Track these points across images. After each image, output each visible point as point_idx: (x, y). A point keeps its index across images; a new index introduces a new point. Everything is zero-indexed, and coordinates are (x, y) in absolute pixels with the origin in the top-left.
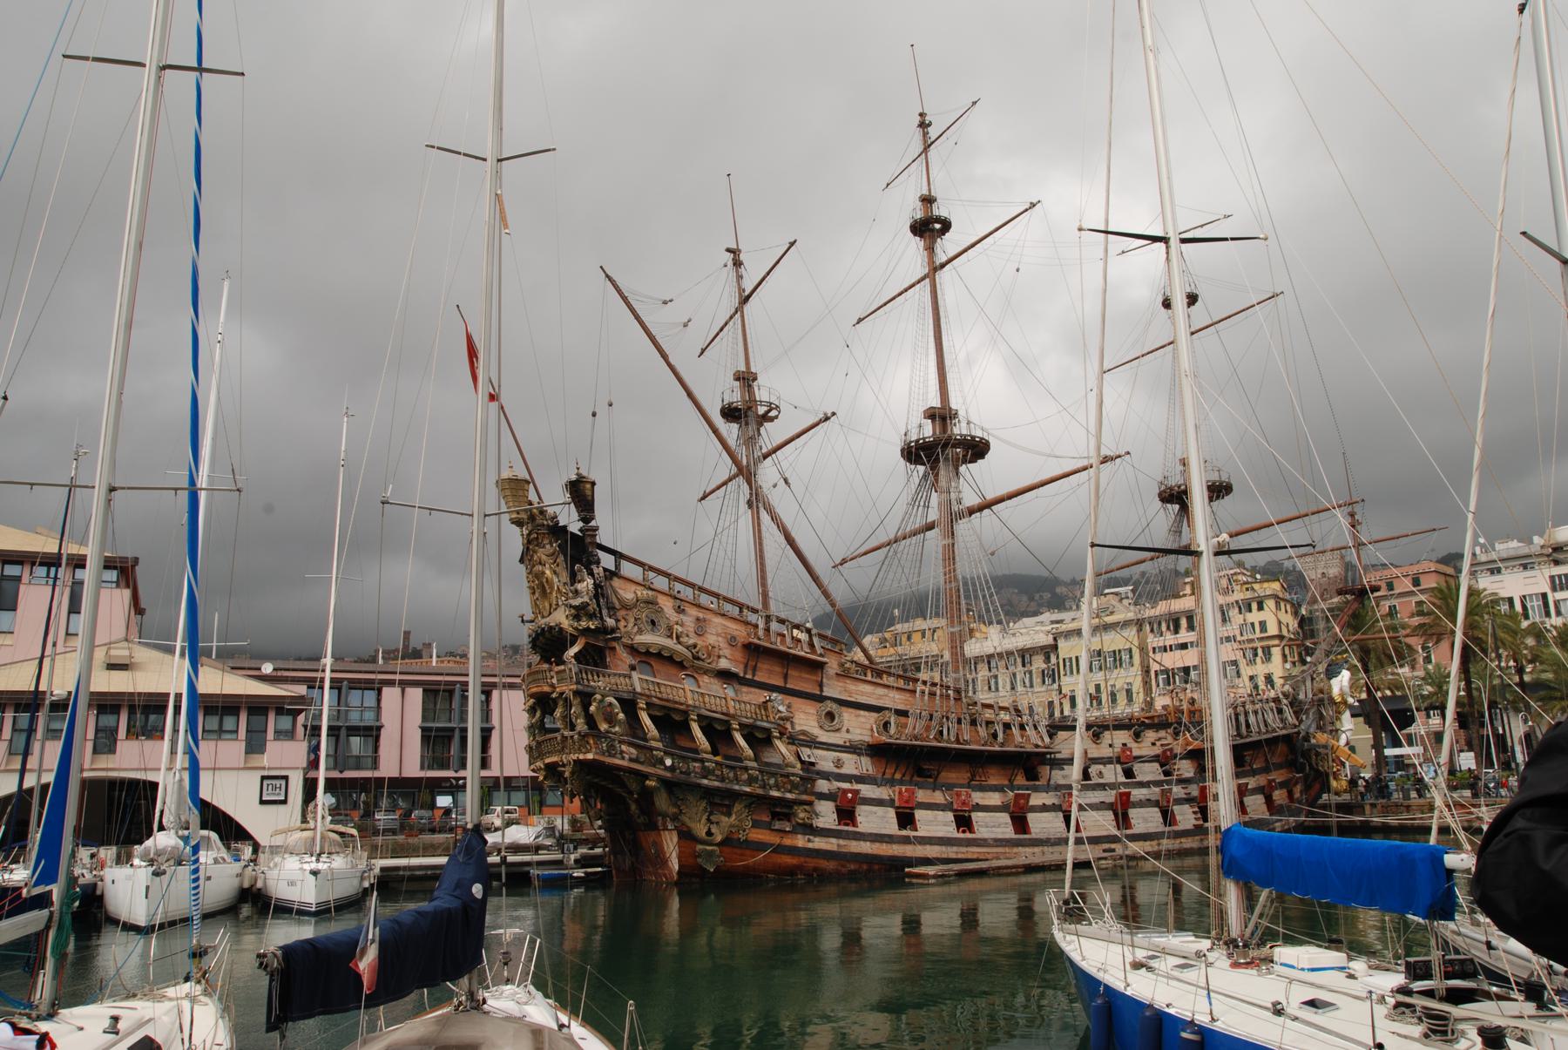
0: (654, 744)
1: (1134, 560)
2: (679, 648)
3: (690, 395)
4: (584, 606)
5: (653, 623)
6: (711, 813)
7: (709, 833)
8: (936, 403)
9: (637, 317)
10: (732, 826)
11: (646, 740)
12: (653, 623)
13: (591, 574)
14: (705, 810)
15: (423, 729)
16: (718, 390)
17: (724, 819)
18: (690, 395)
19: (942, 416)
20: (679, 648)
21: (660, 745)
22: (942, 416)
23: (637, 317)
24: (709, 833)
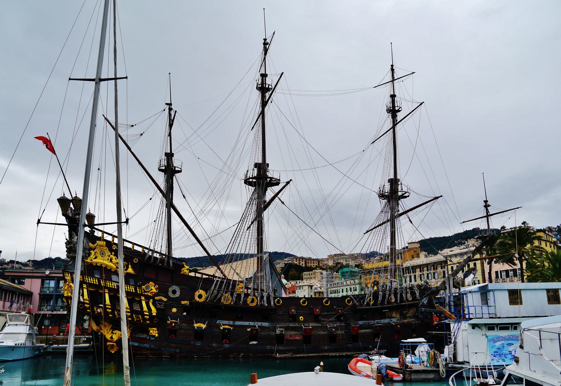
1: (100, 226)
2: (110, 264)
3: (140, 163)
5: (103, 254)
7: (112, 338)
8: (260, 161)
12: (103, 254)
14: (111, 329)
20: (110, 264)
21: (88, 302)
22: (262, 167)
24: (112, 338)
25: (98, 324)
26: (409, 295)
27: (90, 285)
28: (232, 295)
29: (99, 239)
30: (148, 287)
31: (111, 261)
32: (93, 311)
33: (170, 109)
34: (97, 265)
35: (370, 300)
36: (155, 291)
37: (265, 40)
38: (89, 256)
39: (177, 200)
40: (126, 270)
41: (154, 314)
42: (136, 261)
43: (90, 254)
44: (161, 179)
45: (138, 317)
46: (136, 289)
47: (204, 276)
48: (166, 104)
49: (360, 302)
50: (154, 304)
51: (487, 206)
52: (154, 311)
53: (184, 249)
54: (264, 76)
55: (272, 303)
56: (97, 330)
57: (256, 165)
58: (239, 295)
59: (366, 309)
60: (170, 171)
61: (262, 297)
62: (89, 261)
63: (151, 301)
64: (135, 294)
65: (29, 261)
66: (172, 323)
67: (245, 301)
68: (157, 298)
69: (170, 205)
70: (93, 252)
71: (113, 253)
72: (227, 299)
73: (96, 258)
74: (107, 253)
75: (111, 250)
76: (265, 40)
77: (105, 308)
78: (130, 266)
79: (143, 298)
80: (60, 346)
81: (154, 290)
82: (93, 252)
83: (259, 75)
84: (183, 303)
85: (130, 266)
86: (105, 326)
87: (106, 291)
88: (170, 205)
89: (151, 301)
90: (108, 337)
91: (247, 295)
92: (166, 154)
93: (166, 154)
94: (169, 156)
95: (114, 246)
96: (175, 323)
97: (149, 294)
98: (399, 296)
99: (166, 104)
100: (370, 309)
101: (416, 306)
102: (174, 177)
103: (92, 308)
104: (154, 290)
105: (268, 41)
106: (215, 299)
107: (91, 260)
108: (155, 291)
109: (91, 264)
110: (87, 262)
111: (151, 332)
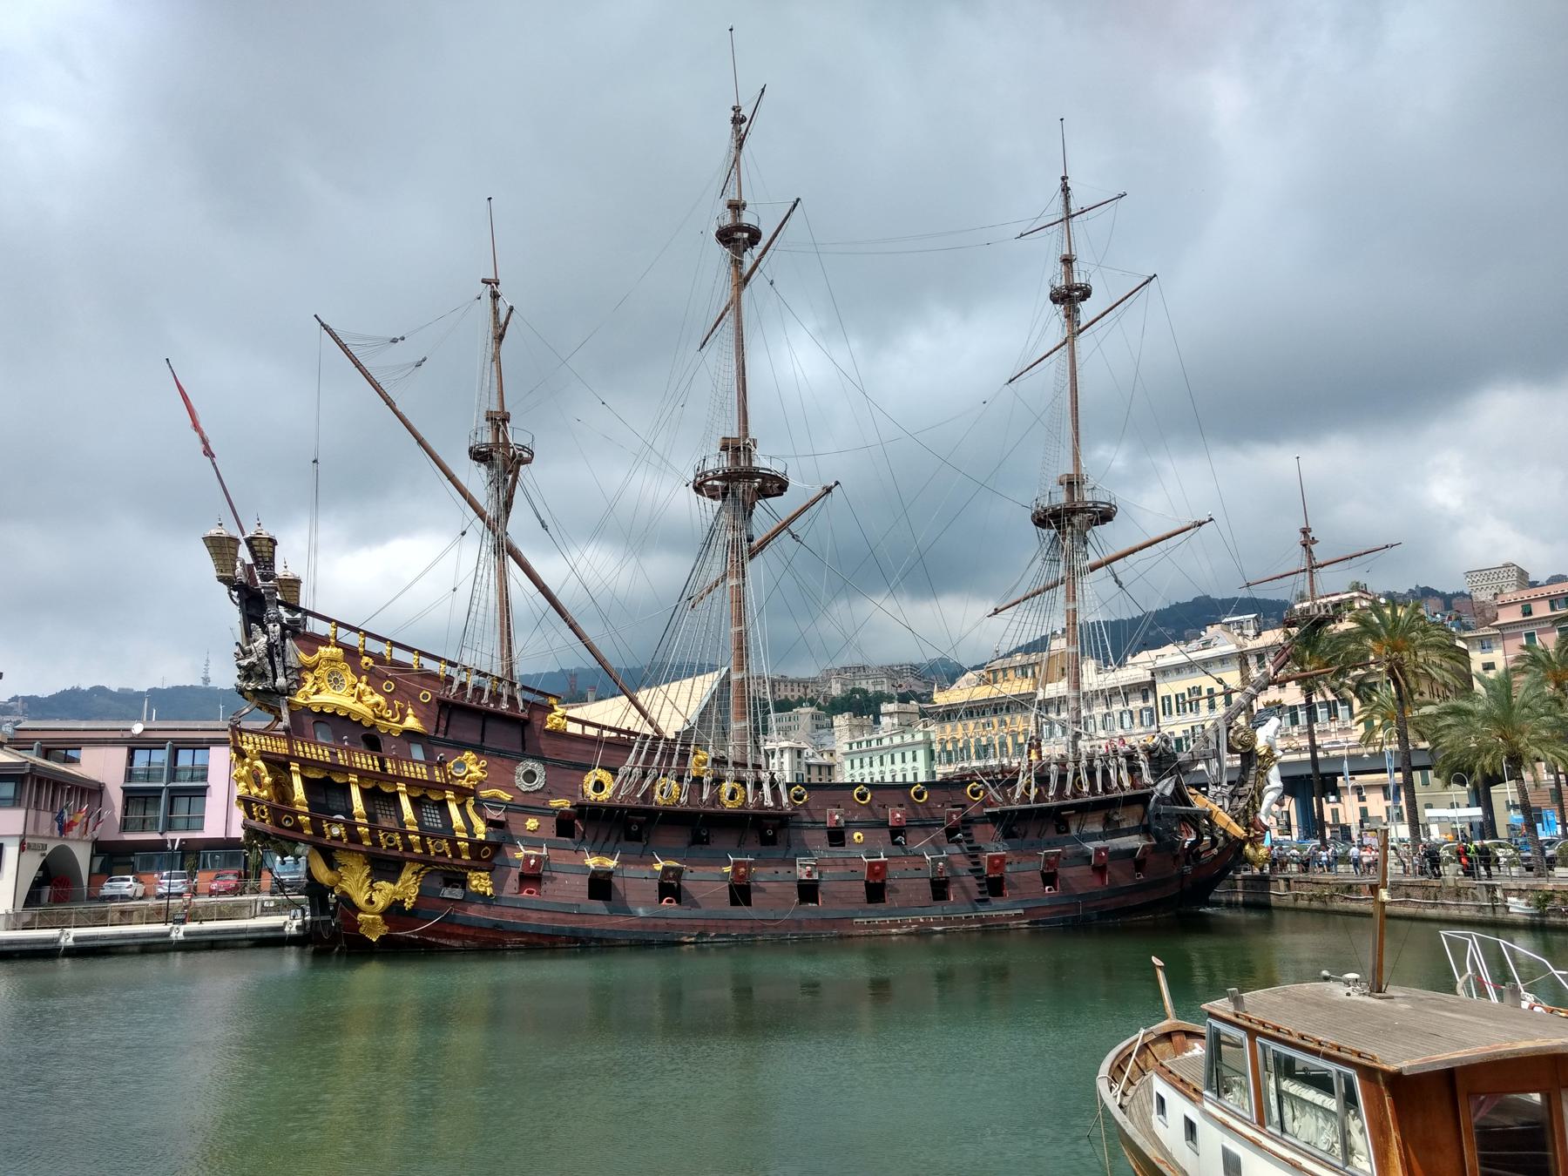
0: (298, 807)
3: (420, 442)
4: (252, 666)
7: (370, 901)
9: (358, 365)
10: (395, 893)
11: (293, 804)
12: (336, 680)
13: (266, 632)
14: (369, 875)
15: (125, 790)
16: (456, 435)
18: (420, 442)
19: (737, 448)
20: (359, 707)
22: (737, 448)
23: (358, 365)
24: (370, 901)
25: (331, 864)
26: (1124, 774)
27: (305, 763)
28: (680, 779)
29: (324, 641)
30: (461, 765)
31: (359, 698)
32: (319, 832)
33: (495, 296)
34: (322, 712)
35: (1028, 788)
36: (479, 774)
37: (736, 109)
38: (300, 687)
40: (401, 721)
41: (482, 837)
42: (426, 696)
43: (300, 682)
44: (477, 479)
45: (439, 847)
46: (431, 773)
47: (606, 734)
48: (484, 281)
49: (1005, 795)
50: (478, 807)
51: (1308, 542)
52: (480, 828)
54: (736, 207)
55: (785, 800)
56: (331, 881)
58: (698, 780)
59: (1020, 811)
61: (758, 785)
62: (299, 699)
63: (471, 800)
64: (431, 785)
66: (528, 858)
67: (715, 798)
68: (485, 793)
69: (505, 550)
70: (310, 678)
71: (364, 678)
72: (668, 792)
73: (318, 692)
74: (349, 678)
75: (358, 672)
76: (736, 109)
77: (351, 827)
78: (410, 711)
79: (450, 795)
81: (476, 772)
82: (310, 678)
83: (723, 203)
84: (554, 803)
85: (410, 711)
86: (351, 871)
87: (353, 778)
89: (471, 800)
90: (360, 899)
91: (718, 781)
93: (490, 417)
94: (499, 420)
95: (366, 659)
96: (538, 858)
97: (464, 783)
98: (1099, 775)
99: (484, 281)
100: (1032, 810)
101: (1144, 799)
103: (316, 824)
104: (476, 772)
105: (746, 112)
106: (636, 790)
107: (307, 698)
108: (479, 774)
109: (307, 709)
110: (297, 704)
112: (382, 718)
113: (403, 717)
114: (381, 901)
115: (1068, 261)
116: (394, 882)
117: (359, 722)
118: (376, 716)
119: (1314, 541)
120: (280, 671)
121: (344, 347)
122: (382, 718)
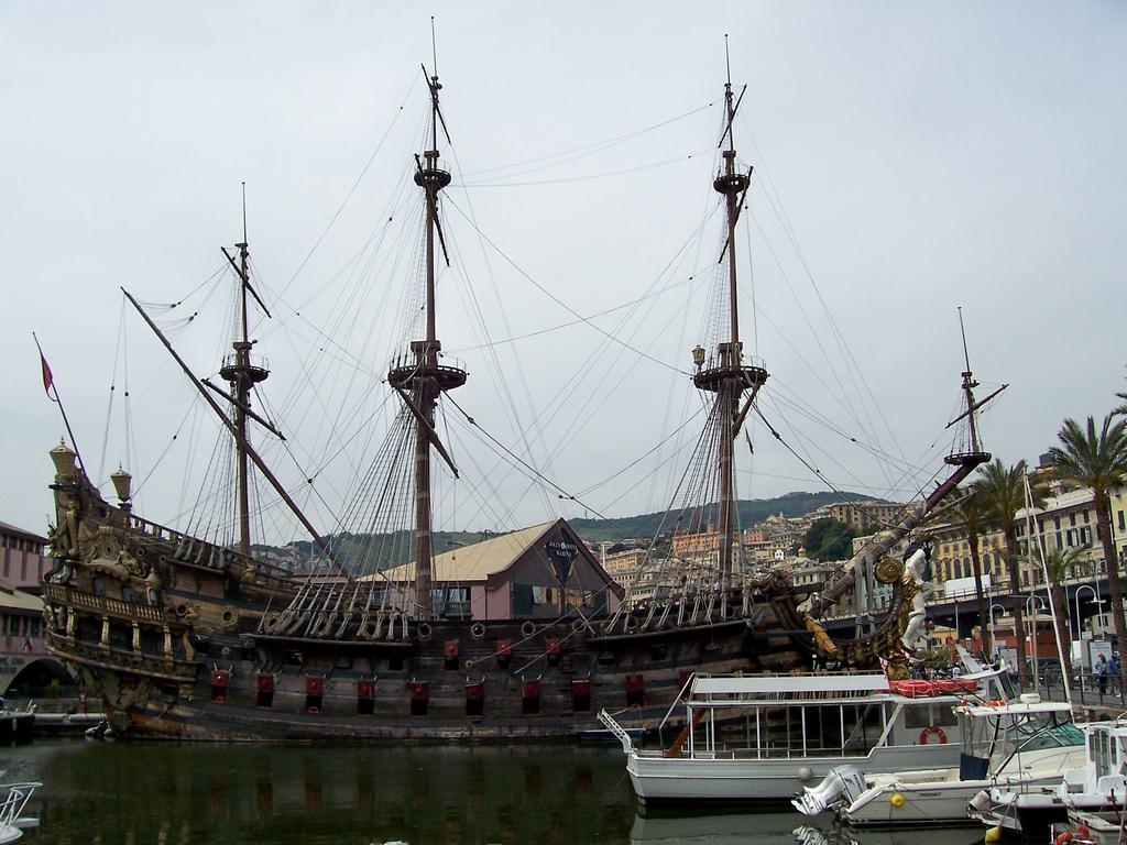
5: (109, 549)
6: (122, 688)
7: (118, 702)
9: (147, 319)
12: (109, 549)
16: (210, 360)
17: (130, 692)
18: (186, 370)
23: (147, 319)
24: (118, 702)
39: (256, 435)
53: (275, 530)
57: (417, 348)
60: (244, 375)
65: (290, 544)
69: (245, 449)
80: (89, 715)
88: (245, 449)
92: (236, 345)
93: (236, 345)
94: (243, 348)
102: (251, 391)
111: (181, 691)
112: (134, 574)
113: (148, 573)
114: (125, 702)
115: (729, 156)
116: (134, 690)
117: (119, 578)
118: (130, 574)
119: (976, 384)
120: (74, 542)
121: (138, 307)
122: (134, 574)
